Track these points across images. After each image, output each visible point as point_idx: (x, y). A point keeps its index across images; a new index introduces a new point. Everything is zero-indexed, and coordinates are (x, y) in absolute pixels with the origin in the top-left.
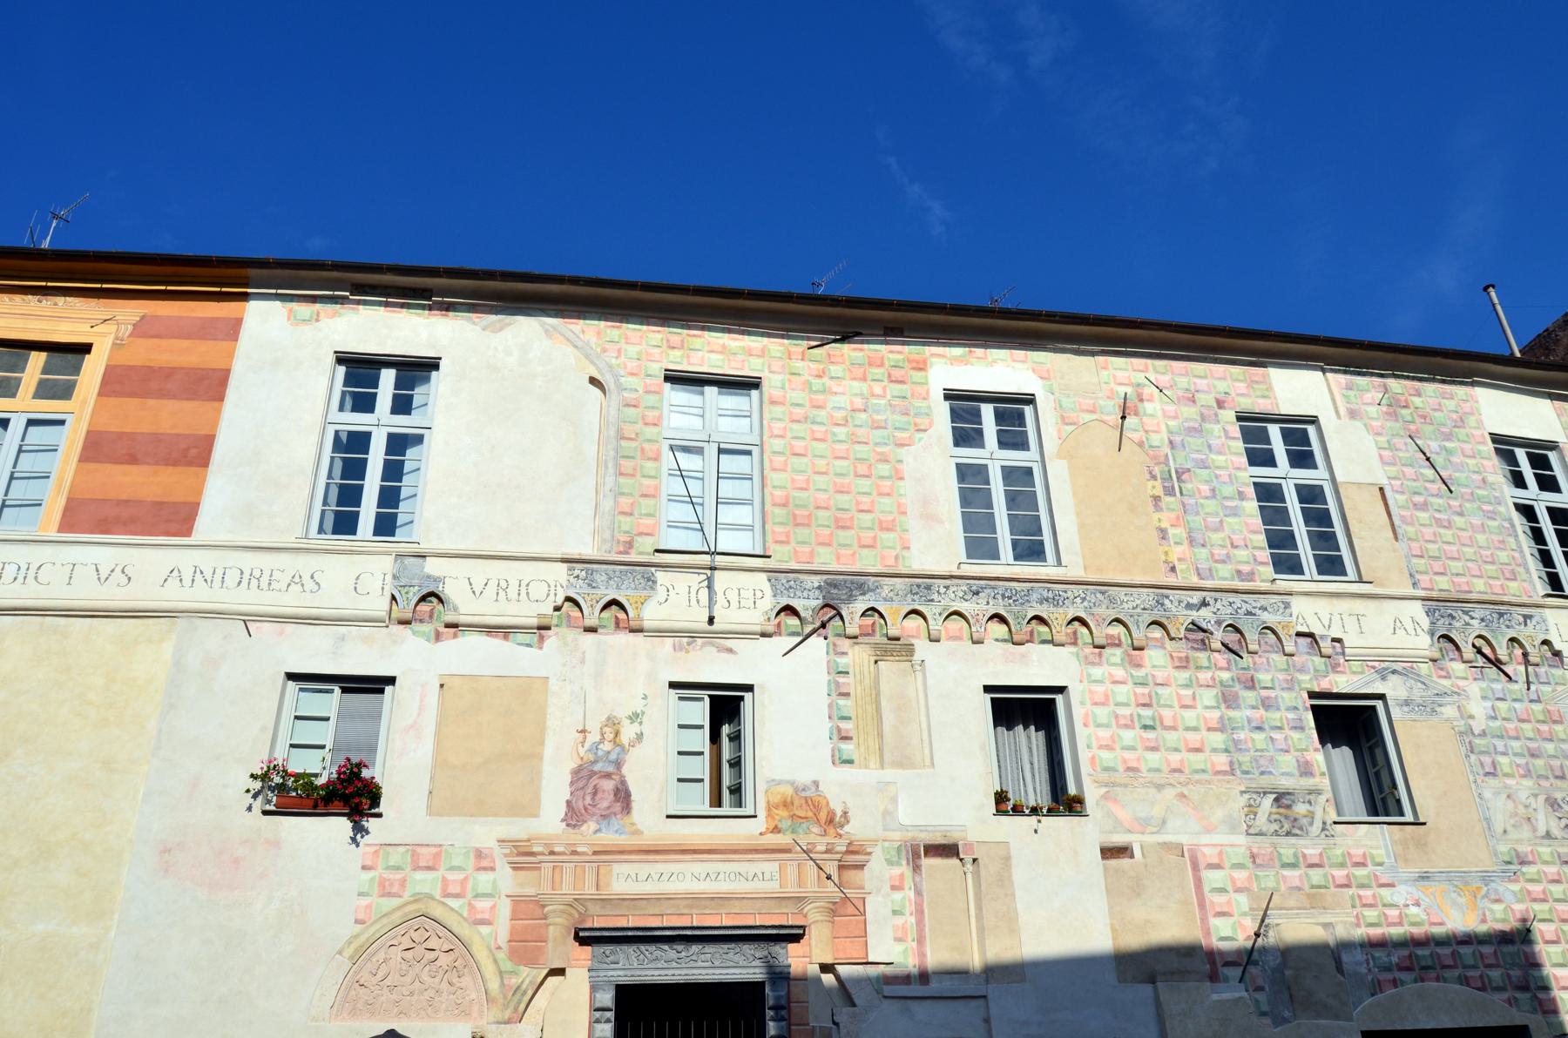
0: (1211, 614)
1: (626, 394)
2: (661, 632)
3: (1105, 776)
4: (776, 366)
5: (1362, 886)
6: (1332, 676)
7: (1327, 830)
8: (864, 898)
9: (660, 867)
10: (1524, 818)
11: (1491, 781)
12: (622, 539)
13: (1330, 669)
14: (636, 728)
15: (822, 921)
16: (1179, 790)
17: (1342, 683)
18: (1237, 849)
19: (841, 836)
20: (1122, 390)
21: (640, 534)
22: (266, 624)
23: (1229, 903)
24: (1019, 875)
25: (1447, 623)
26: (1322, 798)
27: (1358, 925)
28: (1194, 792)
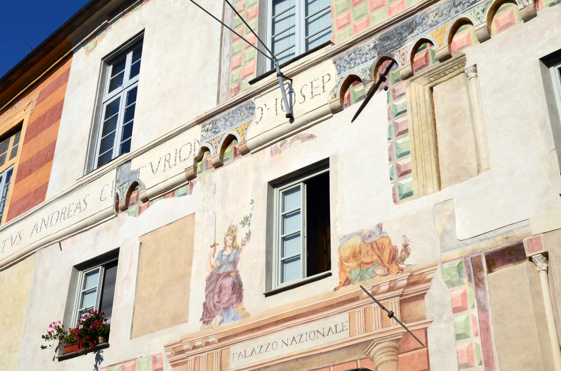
2: (261, 146)
8: (426, 329)
9: (261, 341)
14: (246, 229)
15: (387, 361)
19: (402, 270)
22: (68, 240)
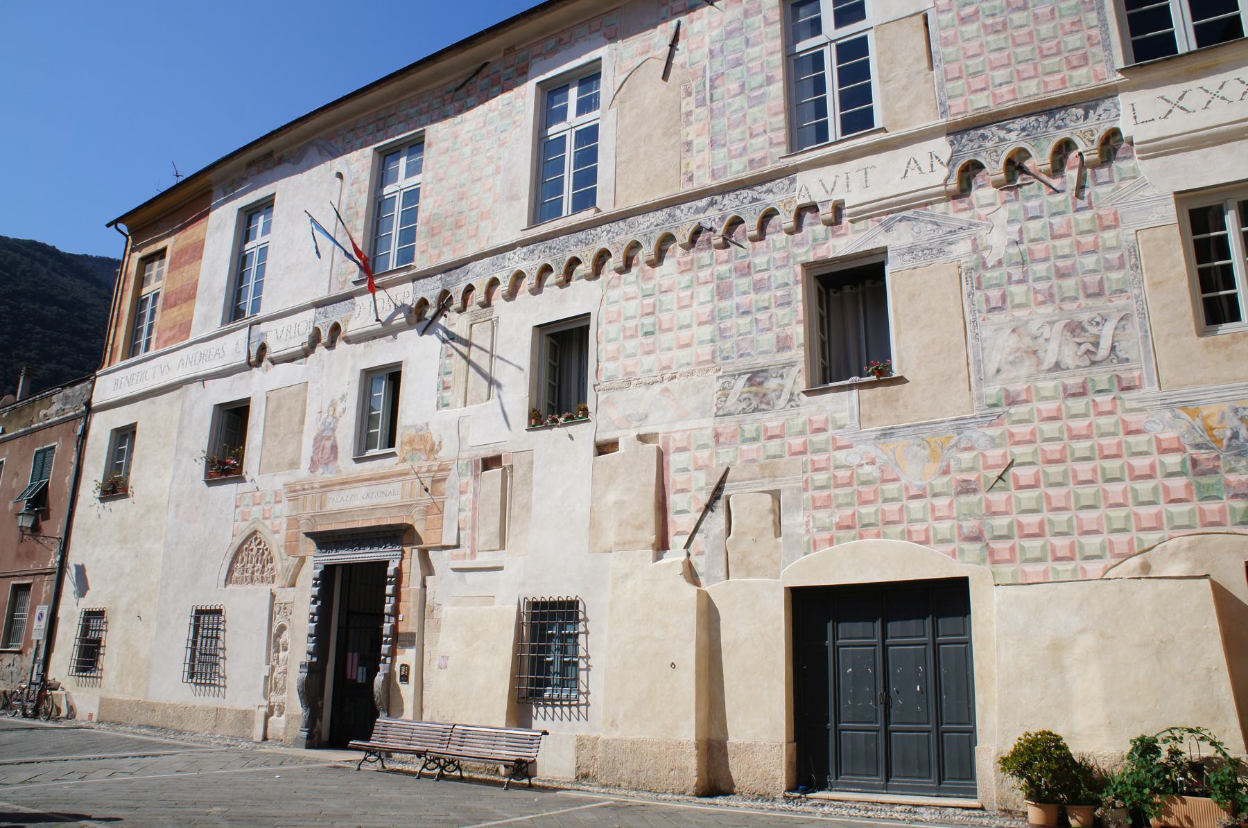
0: (717, 212)
5: (818, 451)
6: (832, 242)
7: (794, 400)
9: (348, 493)
10: (1027, 352)
11: (996, 317)
13: (830, 235)
23: (689, 480)
25: (976, 146)
26: (796, 369)
27: (806, 489)
28: (674, 386)
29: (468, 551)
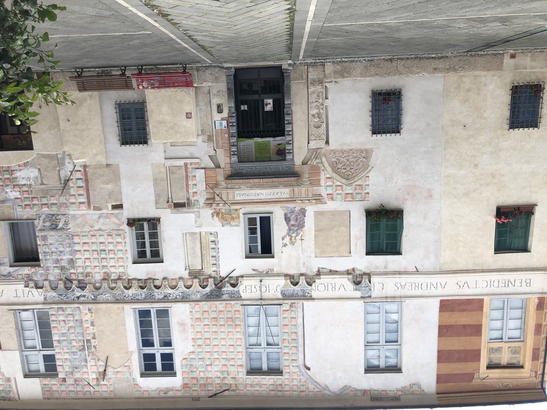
0: (76, 294)
1: (296, 364)
3: (120, 232)
4: (241, 381)
6: (30, 273)
9: (274, 197)
12: (294, 308)
14: (285, 242)
16: (93, 229)
17: (26, 270)
18: (74, 209)
19: (214, 209)
20: (105, 382)
21: (287, 311)
23: (78, 191)
24: (153, 198)
26: (39, 228)
28: (87, 229)
29: (189, 166)
